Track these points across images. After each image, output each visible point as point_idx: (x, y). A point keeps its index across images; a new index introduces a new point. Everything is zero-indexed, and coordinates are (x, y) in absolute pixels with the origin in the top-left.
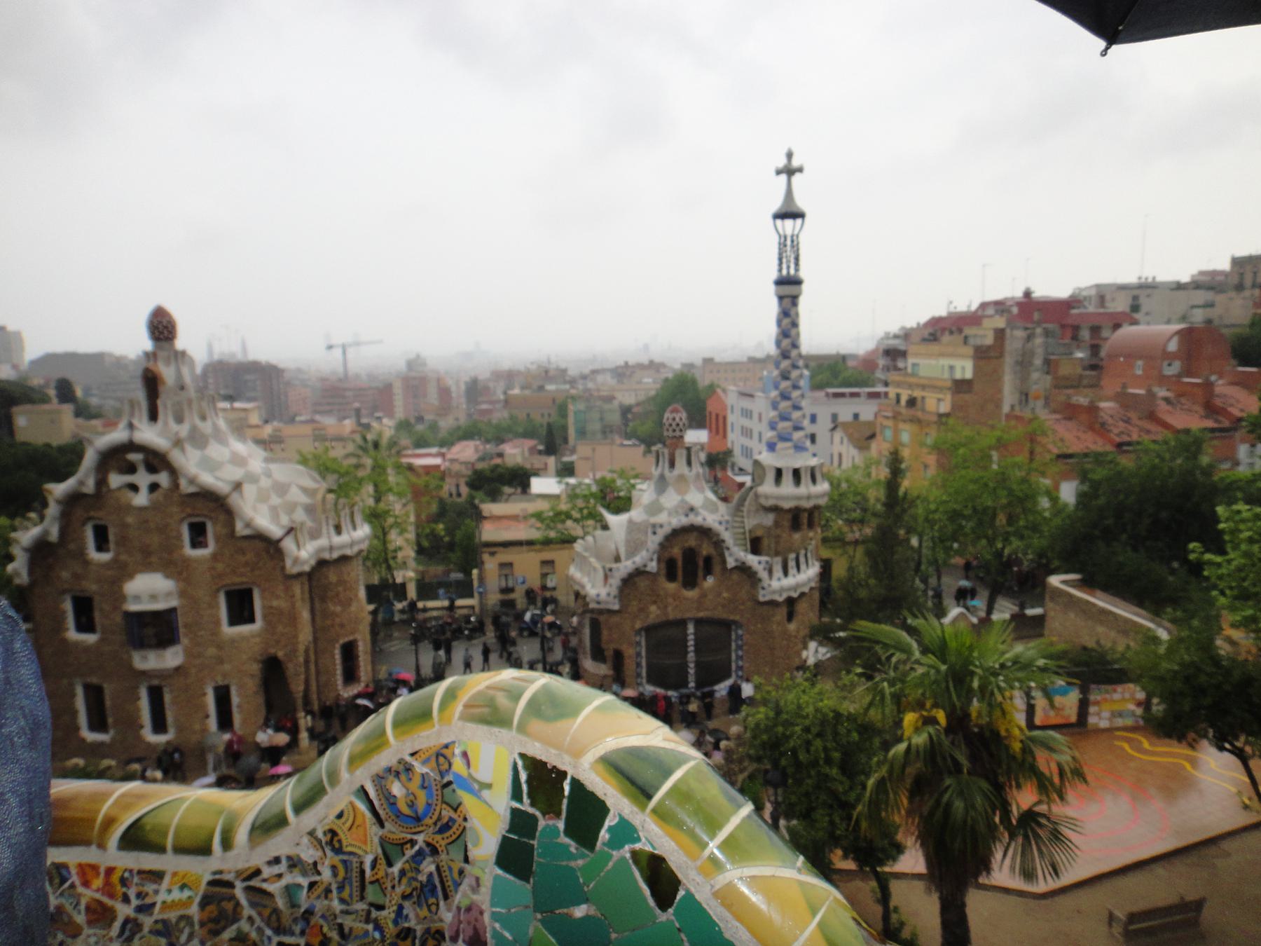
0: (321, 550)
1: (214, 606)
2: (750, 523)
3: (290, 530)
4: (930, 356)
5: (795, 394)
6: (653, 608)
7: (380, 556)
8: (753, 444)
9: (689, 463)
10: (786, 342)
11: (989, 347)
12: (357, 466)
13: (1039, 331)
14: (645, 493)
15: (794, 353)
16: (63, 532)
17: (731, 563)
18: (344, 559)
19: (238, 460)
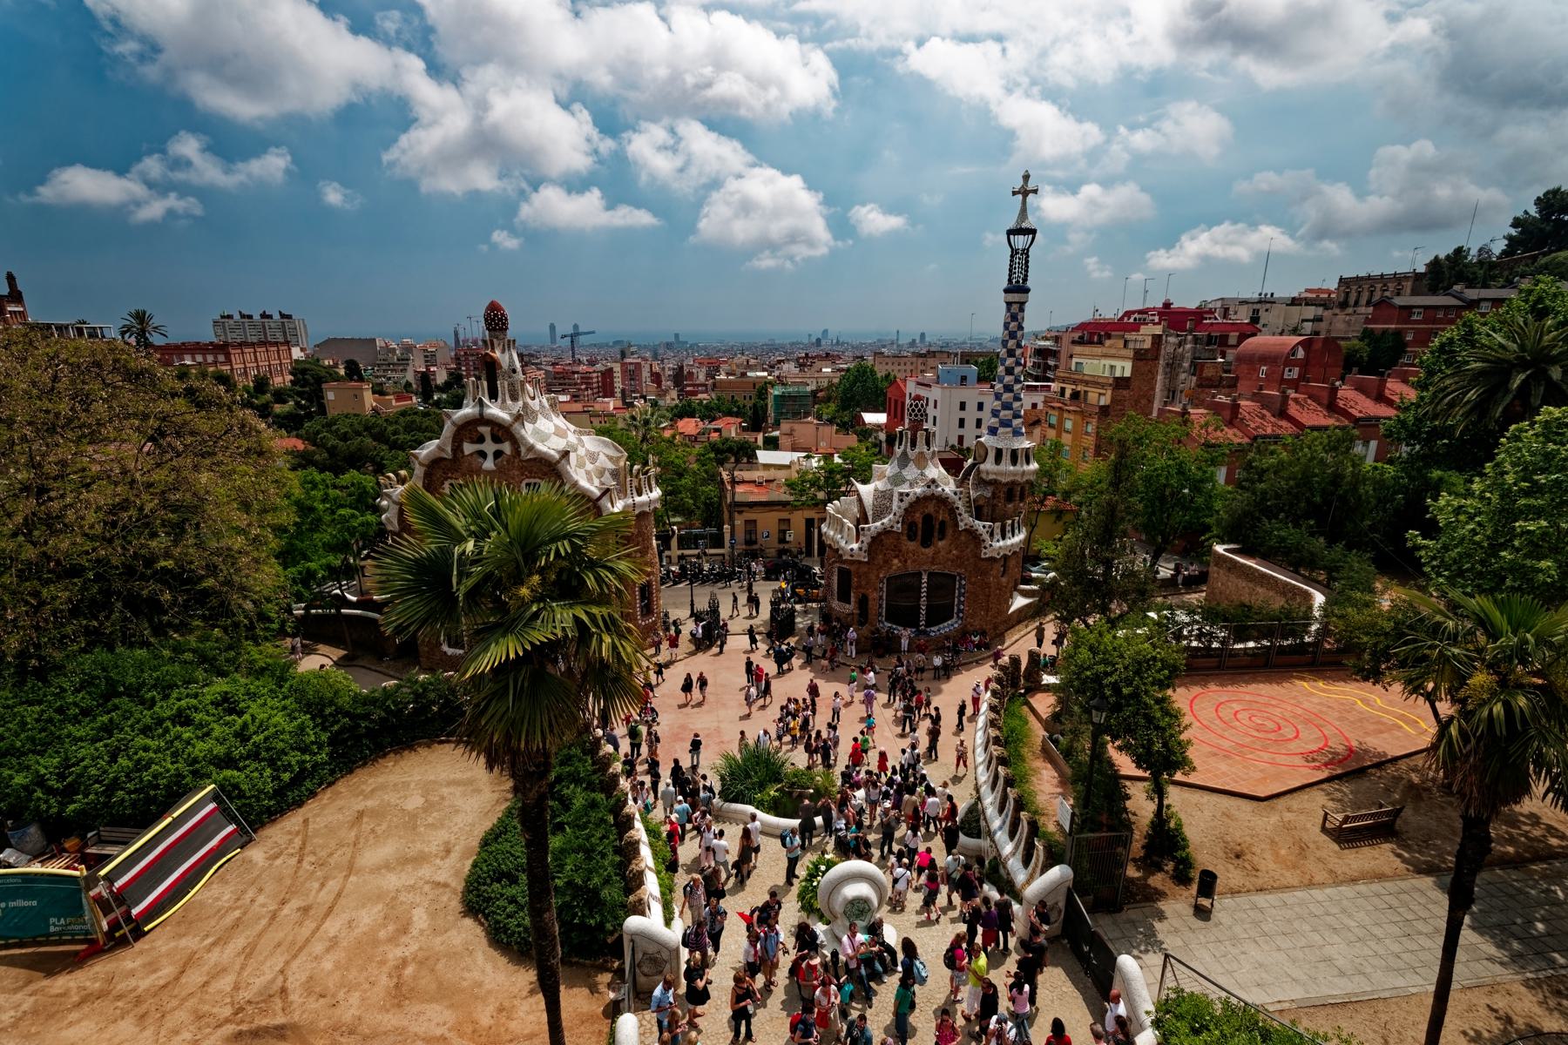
6: (896, 561)
9: (928, 444)
17: (962, 526)
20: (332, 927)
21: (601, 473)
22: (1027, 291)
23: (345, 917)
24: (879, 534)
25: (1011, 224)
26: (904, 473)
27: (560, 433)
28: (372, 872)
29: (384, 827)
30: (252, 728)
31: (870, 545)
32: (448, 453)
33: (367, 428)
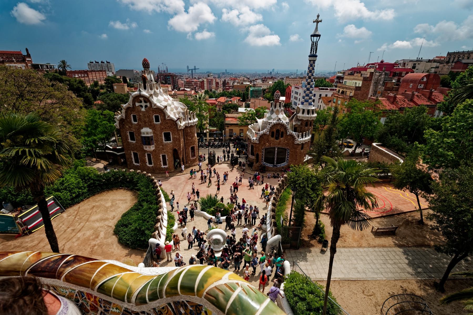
0: (186, 124)
1: (161, 136)
2: (294, 123)
3: (178, 119)
4: (350, 79)
5: (311, 89)
6: (267, 144)
7: (200, 126)
8: (297, 101)
9: (280, 107)
10: (310, 74)
11: (368, 77)
12: (195, 103)
13: (383, 73)
14: (267, 115)
15: (312, 77)
16: (126, 116)
18: (191, 126)
19: (166, 100)
20: (79, 235)
21: (179, 113)
22: (316, 56)
23: (83, 233)
24: (262, 135)
25: (312, 33)
26: (272, 116)
27: (166, 100)
28: (93, 222)
29: (99, 210)
30: (65, 181)
31: (259, 138)
32: (131, 106)
33: (118, 98)
